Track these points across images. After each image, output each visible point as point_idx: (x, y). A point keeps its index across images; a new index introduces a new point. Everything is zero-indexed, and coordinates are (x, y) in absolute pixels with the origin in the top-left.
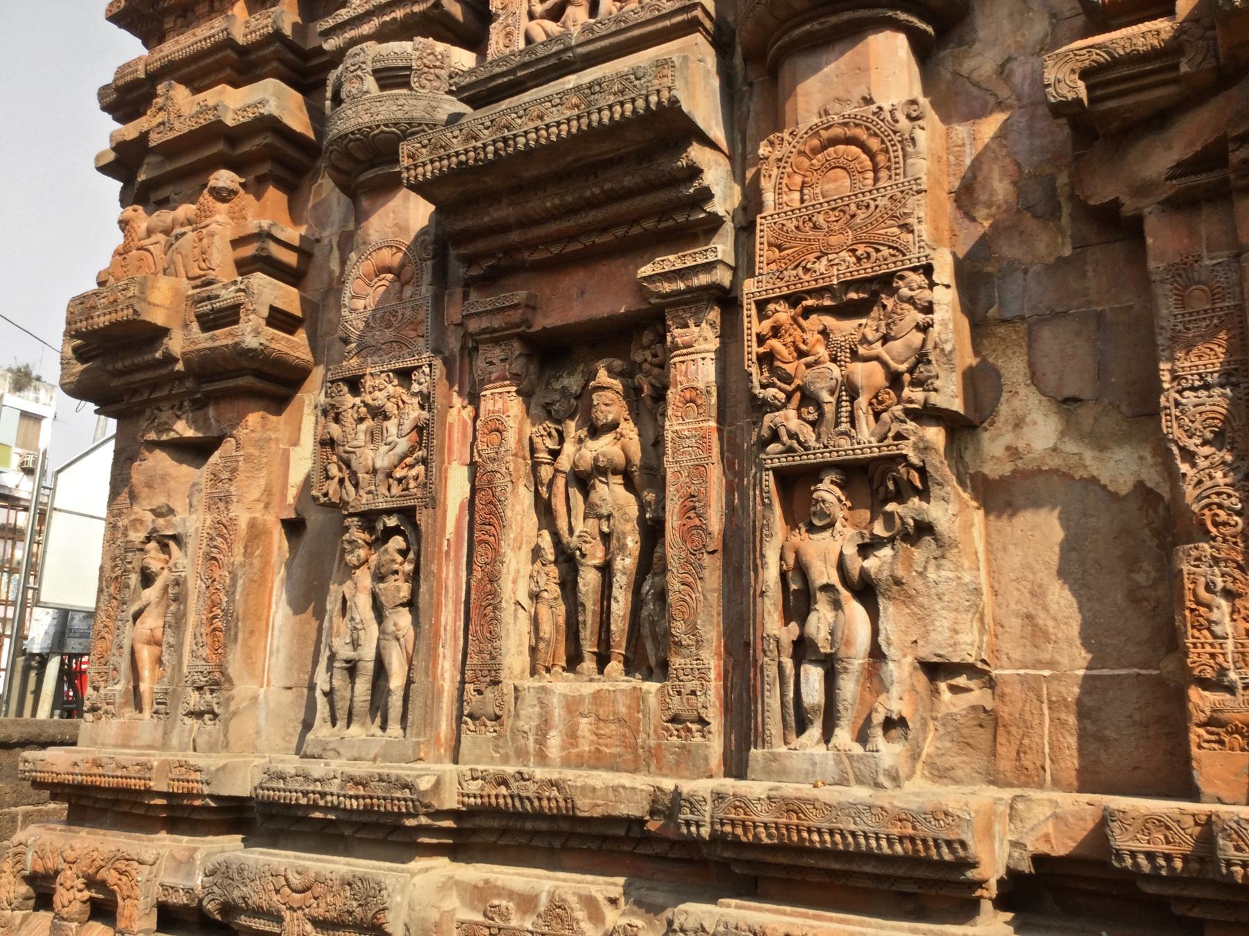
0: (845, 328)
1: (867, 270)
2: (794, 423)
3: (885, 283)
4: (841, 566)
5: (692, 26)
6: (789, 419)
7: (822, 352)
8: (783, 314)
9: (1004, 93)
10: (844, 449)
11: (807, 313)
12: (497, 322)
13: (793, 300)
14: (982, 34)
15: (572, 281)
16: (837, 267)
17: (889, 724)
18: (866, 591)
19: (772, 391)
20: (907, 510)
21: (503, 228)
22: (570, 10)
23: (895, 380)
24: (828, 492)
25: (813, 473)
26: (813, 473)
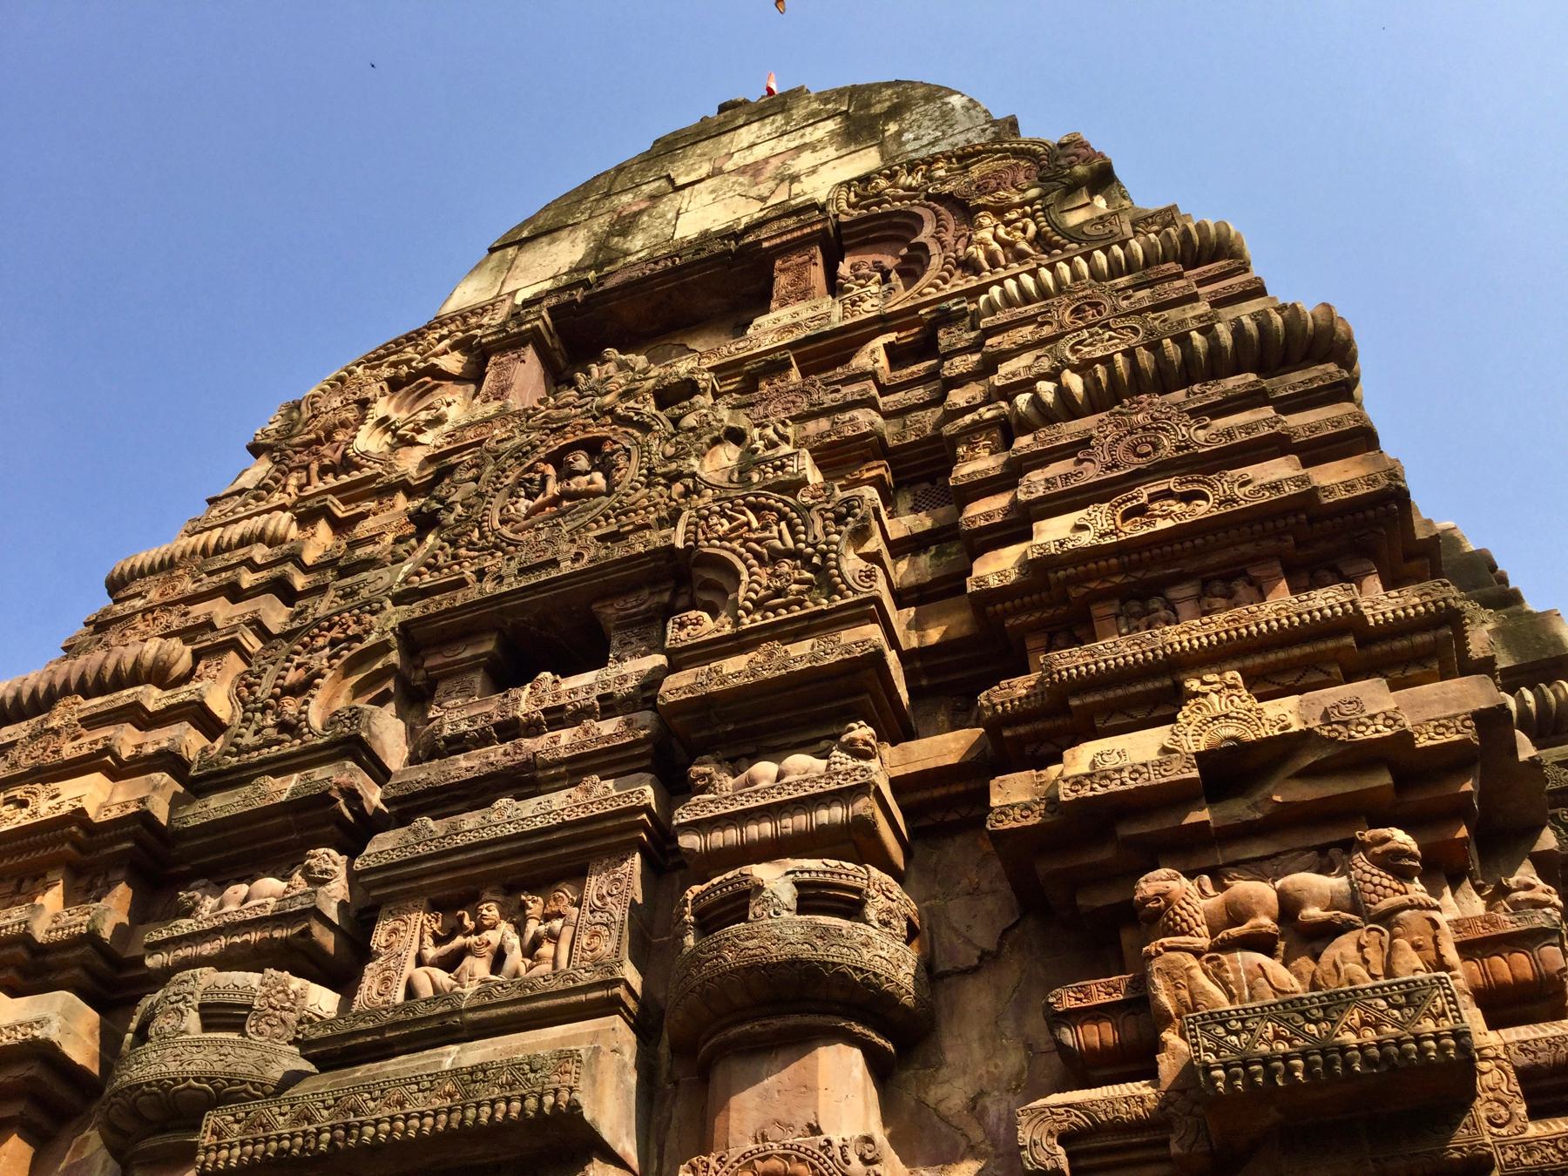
5: (609, 1006)
9: (977, 1135)
14: (950, 1057)
22: (468, 961)
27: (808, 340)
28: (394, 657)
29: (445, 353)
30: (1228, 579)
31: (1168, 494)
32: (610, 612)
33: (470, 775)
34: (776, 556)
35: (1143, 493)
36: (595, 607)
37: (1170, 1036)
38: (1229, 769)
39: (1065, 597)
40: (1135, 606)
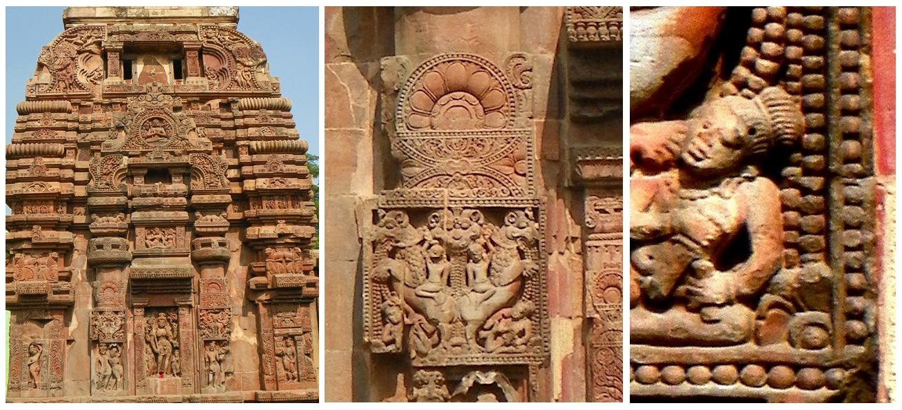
0: (215, 316)
1: (220, 307)
2: (207, 332)
3: (223, 310)
4: (216, 358)
6: (206, 331)
7: (212, 320)
8: (205, 312)
10: (217, 338)
11: (209, 313)
12: (141, 304)
13: (207, 310)
15: (157, 298)
16: (215, 306)
17: (223, 383)
18: (220, 362)
19: (203, 326)
20: (227, 348)
21: (147, 286)
23: (225, 327)
24: (213, 344)
25: (211, 341)
26: (211, 341)
27: (202, 93)
28: (127, 171)
29: (91, 44)
30: (283, 196)
31: (278, 180)
32: (172, 171)
33: (150, 204)
34: (211, 173)
35: (275, 178)
36: (169, 169)
37: (268, 272)
38: (281, 236)
39: (259, 196)
40: (269, 198)
